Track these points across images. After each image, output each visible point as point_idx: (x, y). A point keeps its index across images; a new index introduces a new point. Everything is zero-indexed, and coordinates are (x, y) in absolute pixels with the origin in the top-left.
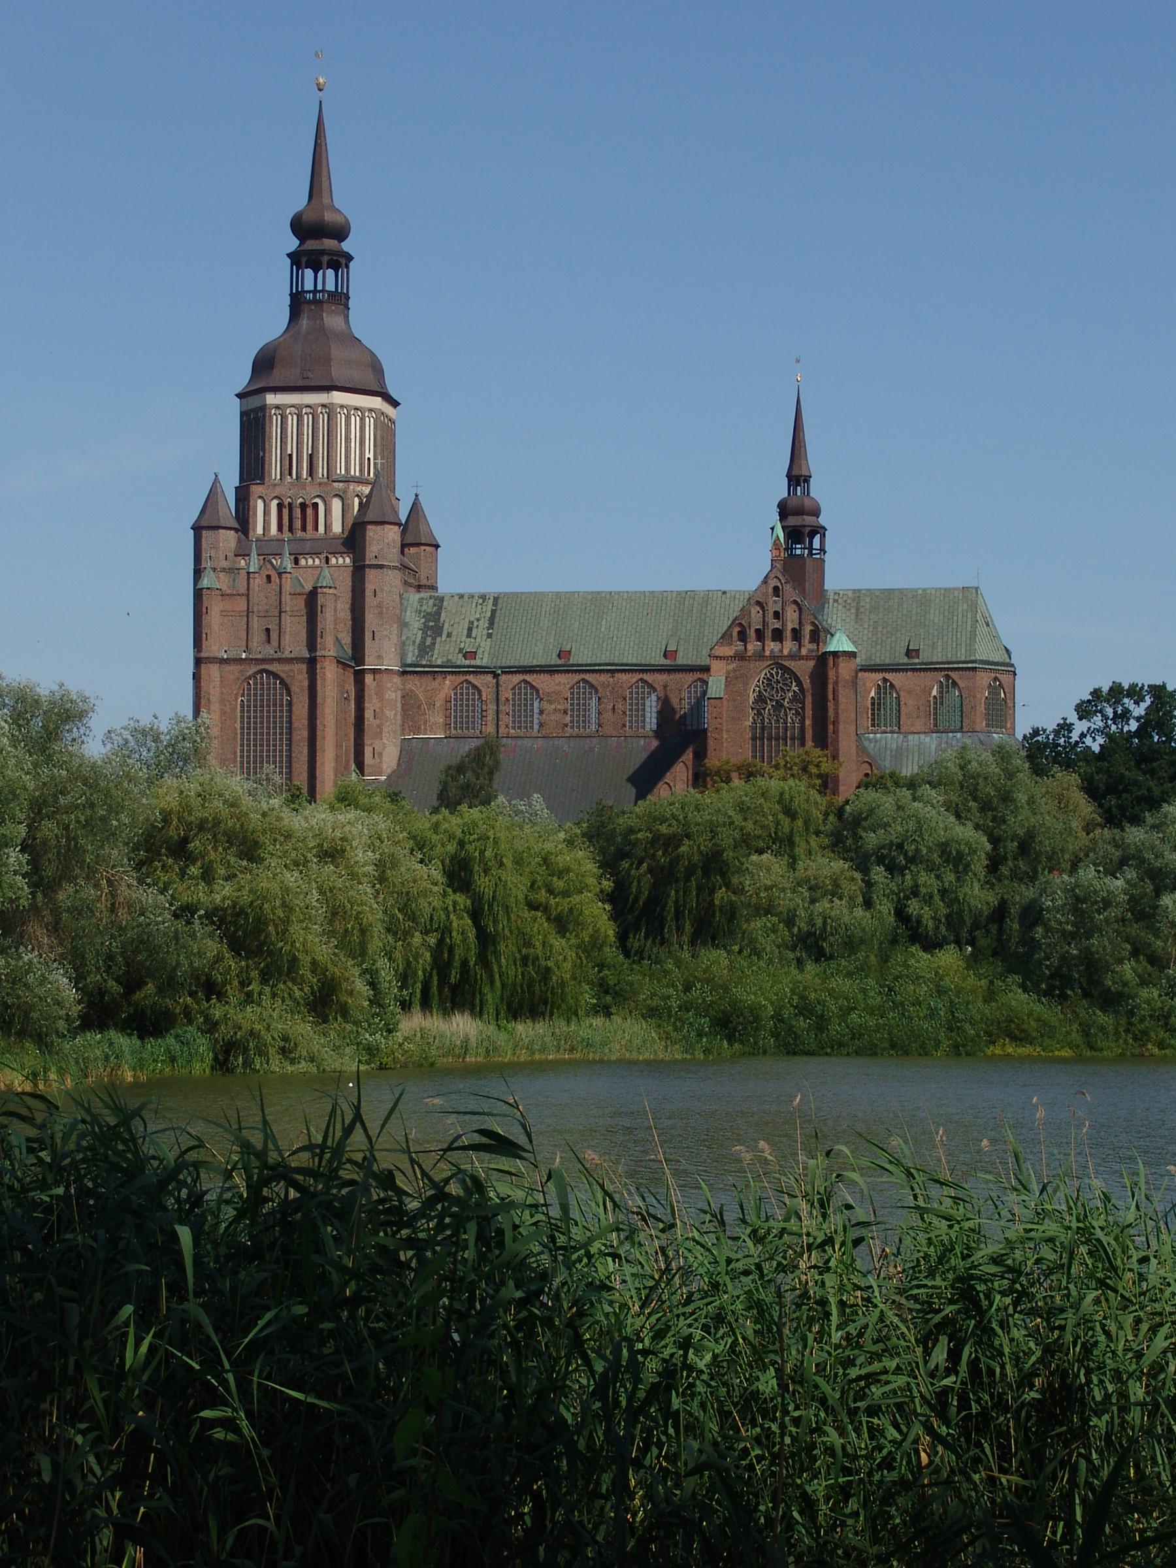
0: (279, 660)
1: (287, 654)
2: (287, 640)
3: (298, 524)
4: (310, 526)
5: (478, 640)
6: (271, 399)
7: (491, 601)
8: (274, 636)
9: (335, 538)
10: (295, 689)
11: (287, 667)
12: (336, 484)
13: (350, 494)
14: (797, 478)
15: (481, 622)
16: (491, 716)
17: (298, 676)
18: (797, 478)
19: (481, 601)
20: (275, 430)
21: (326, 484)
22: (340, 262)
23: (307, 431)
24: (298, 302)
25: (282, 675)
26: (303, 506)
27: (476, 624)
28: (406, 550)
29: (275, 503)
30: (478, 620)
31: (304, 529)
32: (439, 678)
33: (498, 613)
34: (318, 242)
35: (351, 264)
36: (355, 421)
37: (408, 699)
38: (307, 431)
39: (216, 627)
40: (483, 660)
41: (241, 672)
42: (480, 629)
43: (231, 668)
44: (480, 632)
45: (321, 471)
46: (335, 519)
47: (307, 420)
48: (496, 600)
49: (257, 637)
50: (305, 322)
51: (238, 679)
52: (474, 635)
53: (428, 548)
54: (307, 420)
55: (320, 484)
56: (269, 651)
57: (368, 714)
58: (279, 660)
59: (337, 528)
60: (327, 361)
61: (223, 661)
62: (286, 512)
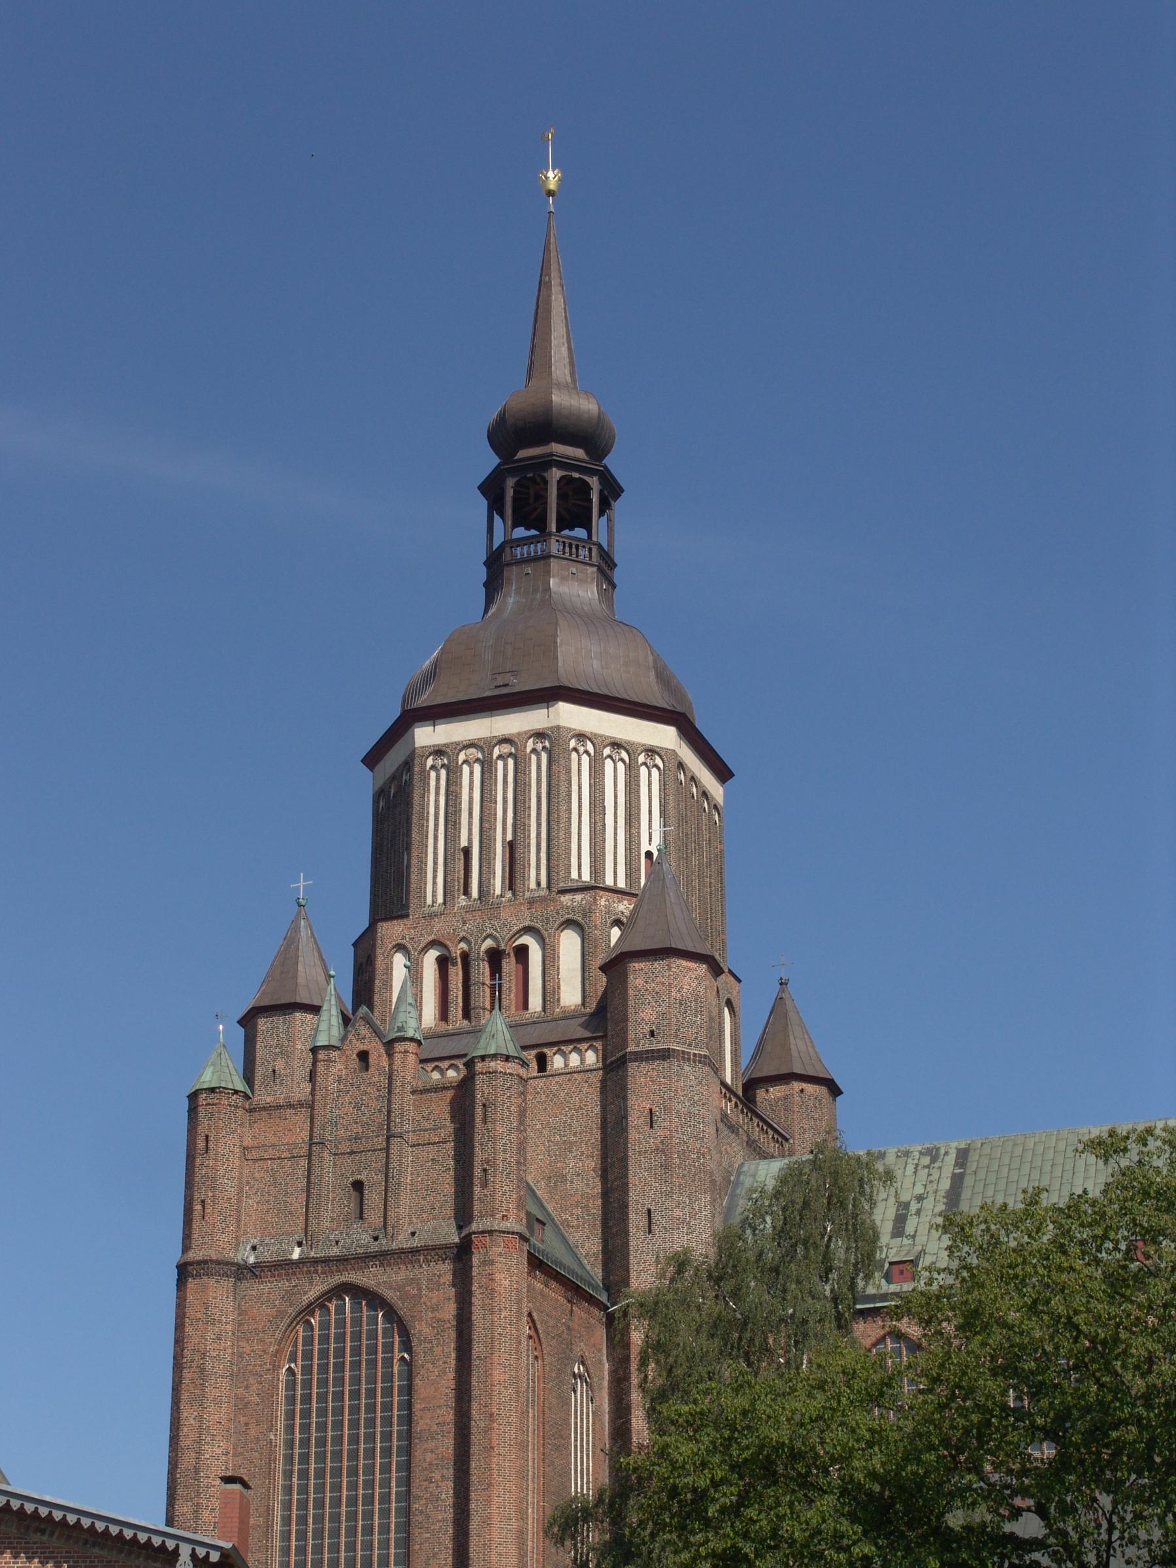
0: (384, 1257)
1: (402, 1241)
2: (405, 1204)
4: (511, 997)
5: (921, 1239)
6: (425, 736)
7: (952, 1158)
8: (373, 1197)
9: (568, 1016)
10: (421, 1328)
12: (566, 899)
13: (598, 918)
15: (928, 1204)
17: (429, 1295)
19: (926, 1160)
20: (434, 801)
21: (543, 900)
23: (504, 792)
25: (388, 1294)
26: (495, 957)
27: (914, 1207)
28: (761, 1094)
29: (432, 955)
30: (920, 1198)
33: (969, 1181)
35: (617, 505)
36: (614, 774)
38: (504, 792)
39: (229, 1186)
41: (288, 1296)
42: (926, 1218)
43: (266, 1287)
45: (535, 875)
46: (565, 973)
47: (504, 771)
49: (334, 1202)
50: (510, 600)
51: (280, 1314)
52: (910, 1228)
53: (810, 1088)
54: (504, 771)
55: (532, 902)
56: (360, 1238)
58: (384, 1257)
59: (570, 995)
60: (549, 649)
61: (242, 1272)
62: (456, 975)
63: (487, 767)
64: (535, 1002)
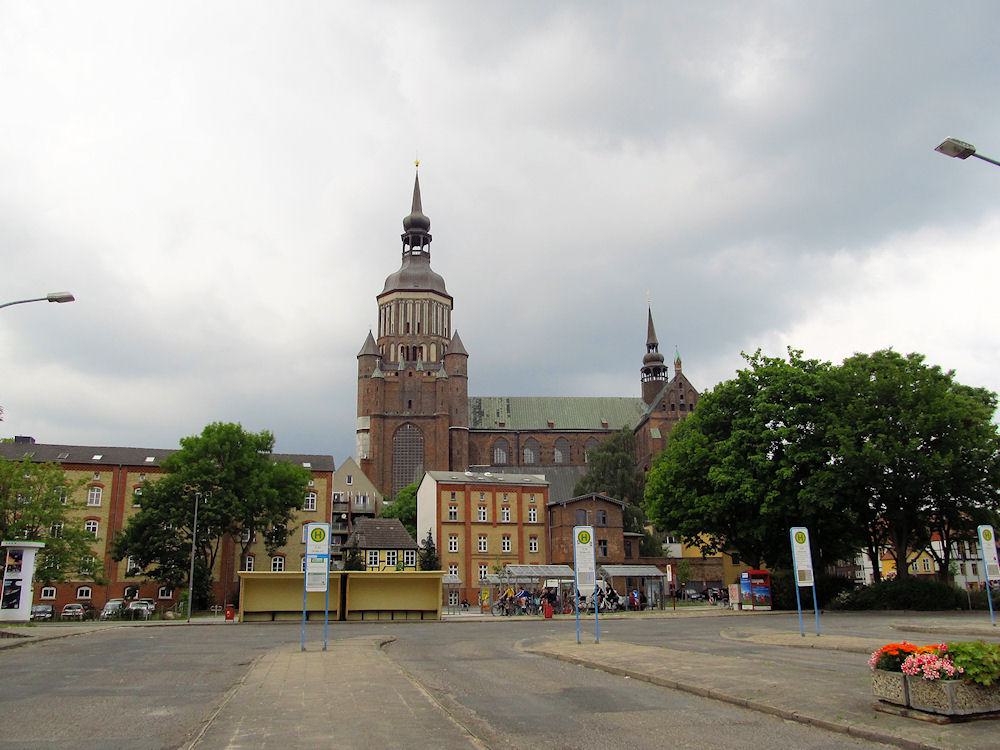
0: (417, 417)
3: (411, 357)
11: (422, 421)
14: (652, 345)
16: (514, 456)
18: (652, 345)
22: (427, 240)
24: (407, 257)
31: (415, 359)
32: (487, 435)
34: (417, 232)
37: (471, 446)
40: (508, 427)
43: (390, 421)
44: (504, 414)
45: (425, 331)
47: (418, 306)
48: (508, 400)
52: (500, 415)
54: (418, 306)
57: (454, 452)
58: (417, 417)
59: (433, 359)
63: (414, 305)
64: (425, 359)
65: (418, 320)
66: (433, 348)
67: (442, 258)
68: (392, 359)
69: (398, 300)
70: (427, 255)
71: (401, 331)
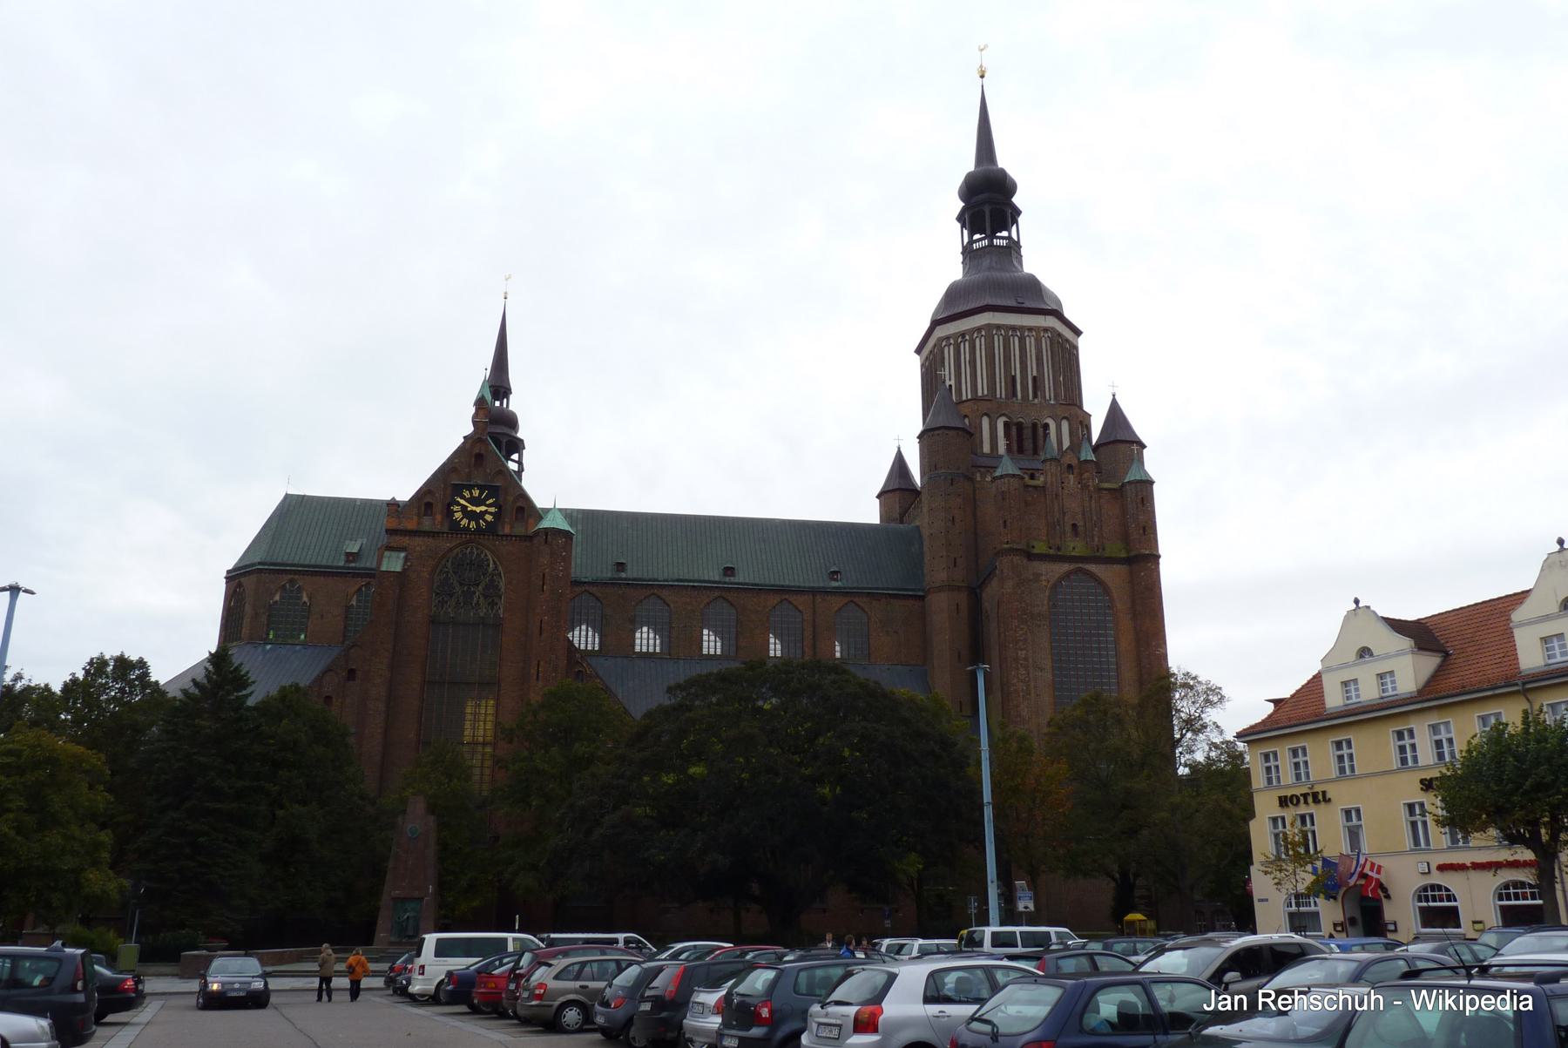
34: (988, 202)
45: (1049, 392)
63: (1022, 340)
65: (1032, 371)
66: (1065, 425)
67: (1042, 252)
68: (986, 449)
69: (989, 327)
70: (1014, 247)
71: (1001, 392)
